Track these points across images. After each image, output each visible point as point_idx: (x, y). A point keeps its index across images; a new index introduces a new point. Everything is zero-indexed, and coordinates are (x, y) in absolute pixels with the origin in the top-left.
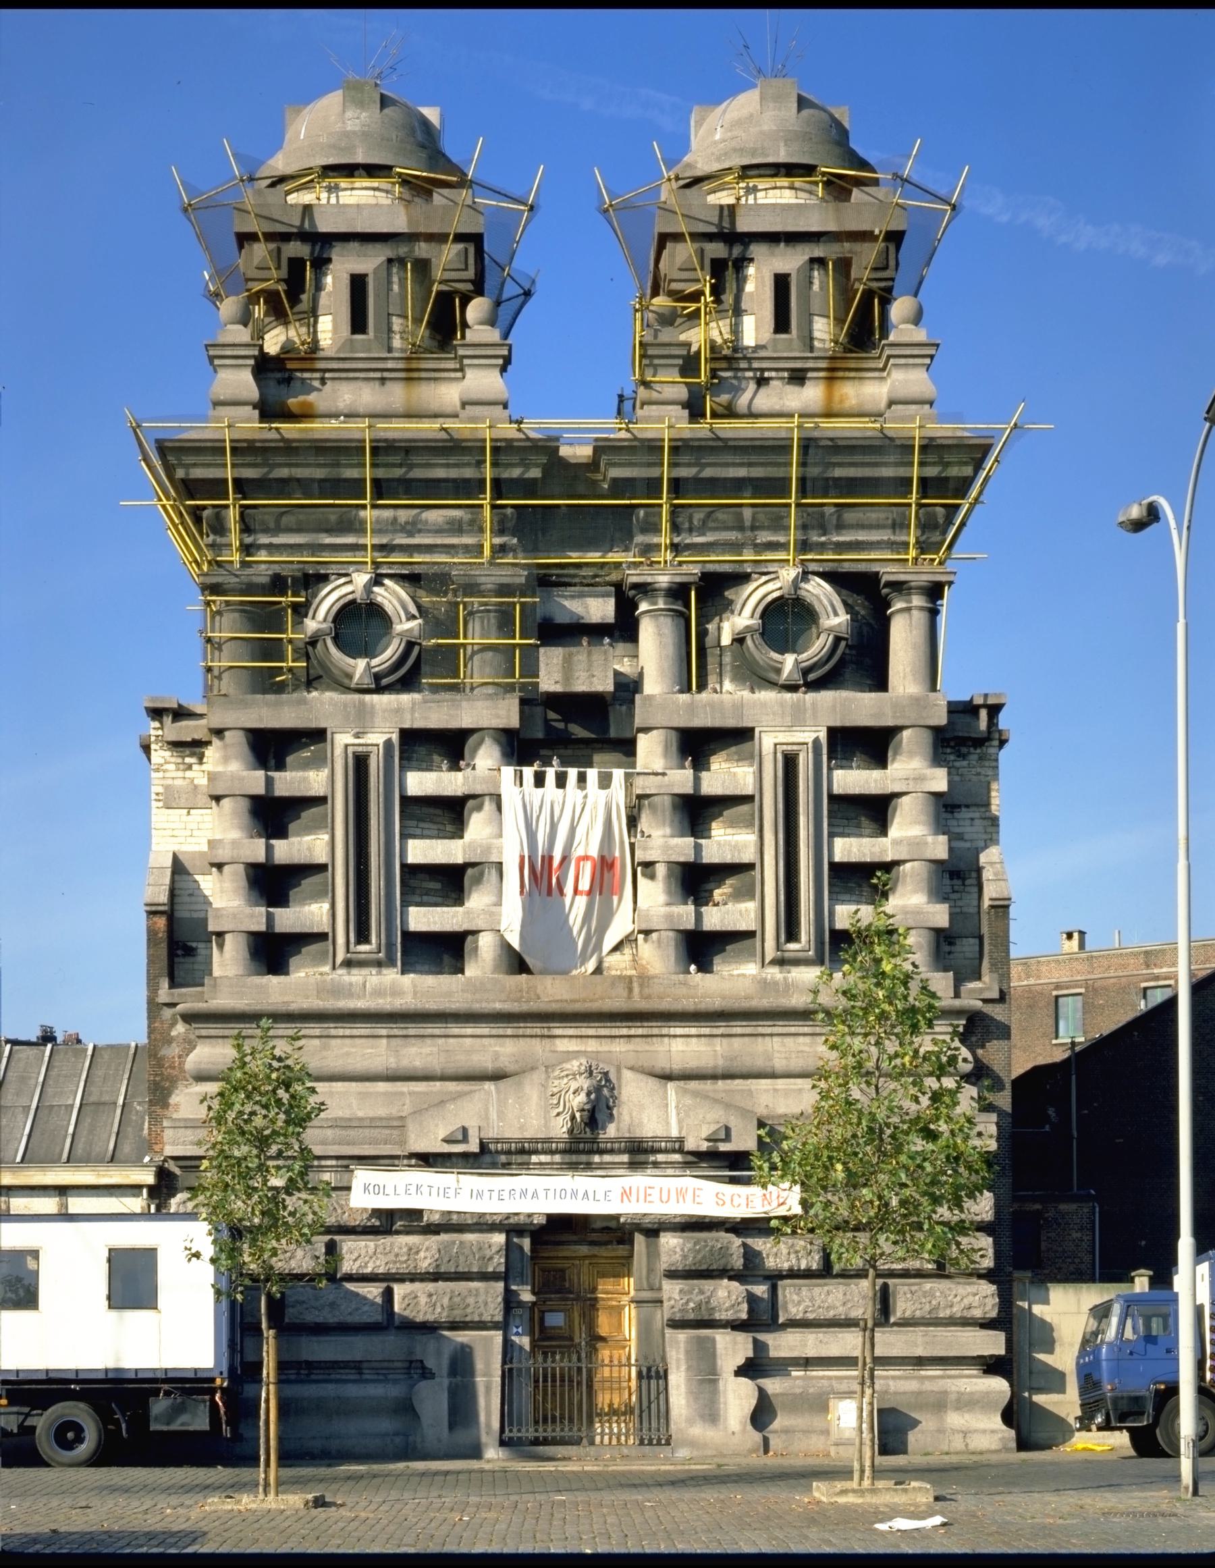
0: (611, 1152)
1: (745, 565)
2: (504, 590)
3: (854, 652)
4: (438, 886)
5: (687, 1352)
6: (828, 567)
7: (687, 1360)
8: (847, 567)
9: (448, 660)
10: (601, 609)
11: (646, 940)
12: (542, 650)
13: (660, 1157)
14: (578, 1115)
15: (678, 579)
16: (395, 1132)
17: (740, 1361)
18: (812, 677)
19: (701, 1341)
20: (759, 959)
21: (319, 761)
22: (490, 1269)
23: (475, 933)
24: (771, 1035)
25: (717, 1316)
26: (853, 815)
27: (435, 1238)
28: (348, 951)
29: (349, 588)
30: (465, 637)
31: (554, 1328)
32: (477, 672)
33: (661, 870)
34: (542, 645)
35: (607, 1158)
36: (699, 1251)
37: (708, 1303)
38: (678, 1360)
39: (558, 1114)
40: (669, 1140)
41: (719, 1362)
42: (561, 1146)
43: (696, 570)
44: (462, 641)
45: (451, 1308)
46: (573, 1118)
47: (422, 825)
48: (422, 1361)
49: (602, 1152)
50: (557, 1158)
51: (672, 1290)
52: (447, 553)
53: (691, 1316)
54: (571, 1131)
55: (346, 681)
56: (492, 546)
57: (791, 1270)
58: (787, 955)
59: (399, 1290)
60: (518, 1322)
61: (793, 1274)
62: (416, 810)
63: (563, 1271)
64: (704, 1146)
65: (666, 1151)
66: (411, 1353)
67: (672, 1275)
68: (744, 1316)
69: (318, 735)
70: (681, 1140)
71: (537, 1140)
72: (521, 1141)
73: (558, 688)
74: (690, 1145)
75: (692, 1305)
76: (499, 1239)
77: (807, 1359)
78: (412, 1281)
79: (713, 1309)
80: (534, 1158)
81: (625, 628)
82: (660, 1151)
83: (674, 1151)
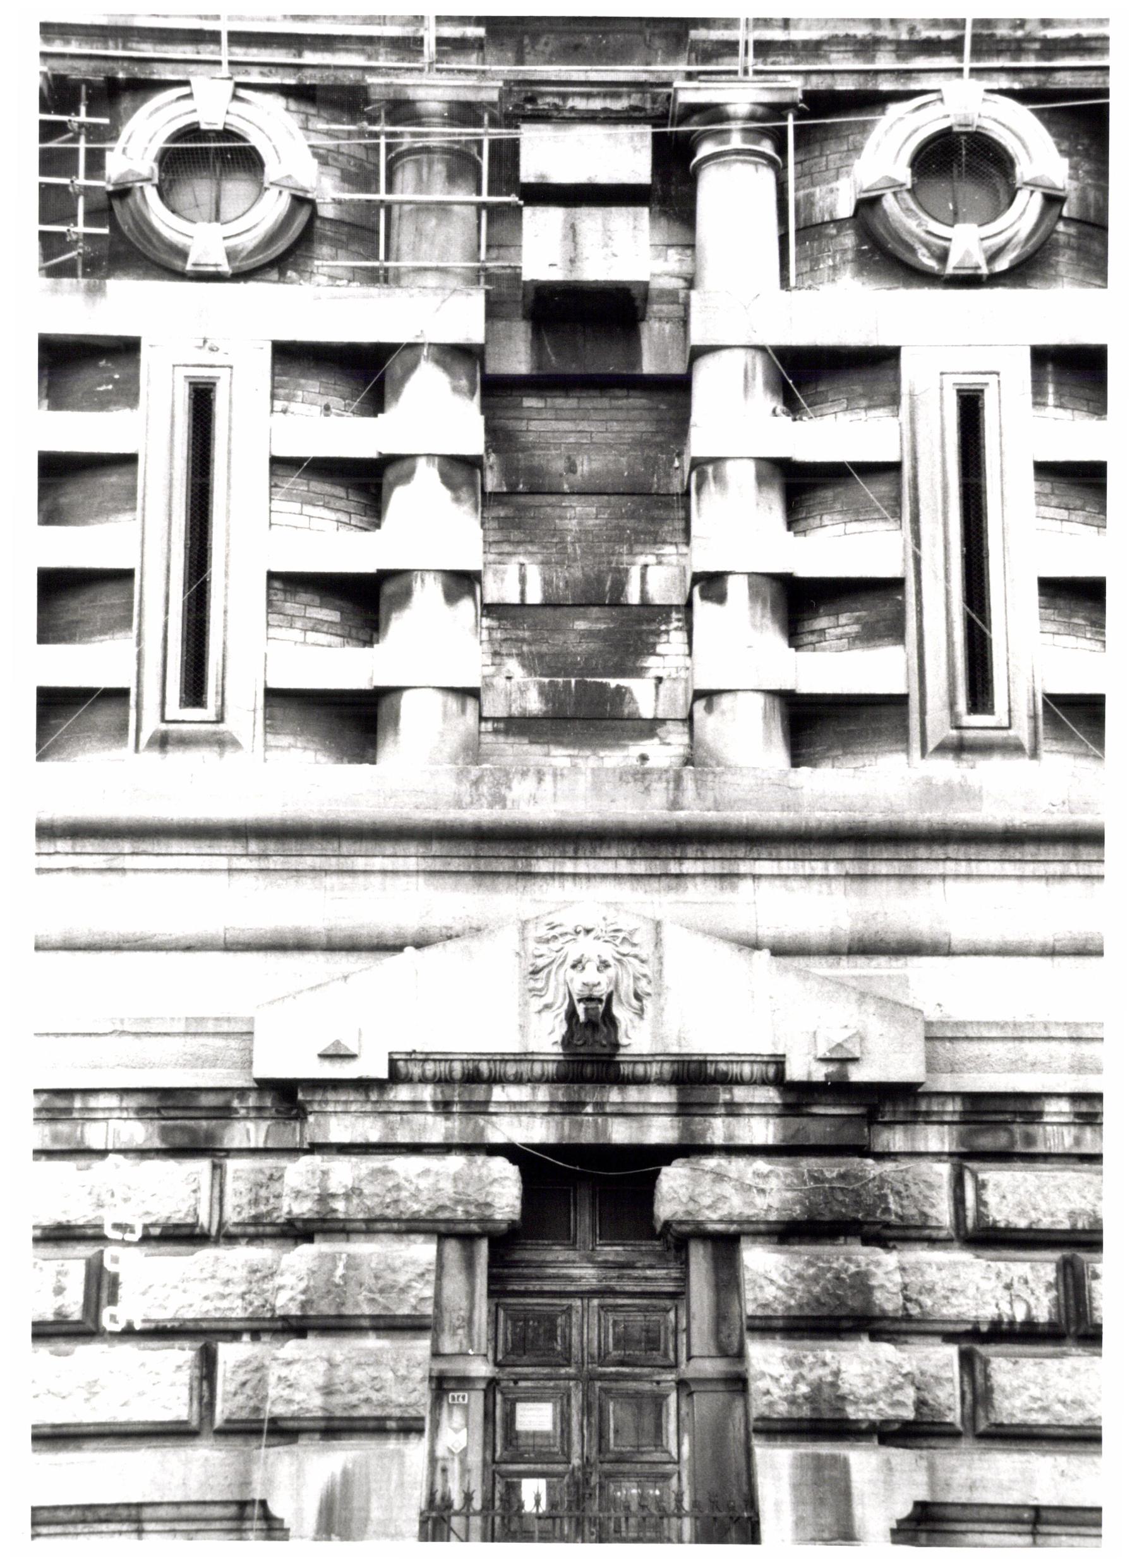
0: (643, 1081)
1: (881, 78)
2: (464, 113)
3: (1072, 230)
4: (334, 616)
5: (796, 1487)
6: (1033, 81)
7: (798, 1502)
8: (1065, 81)
9: (362, 232)
10: (627, 156)
11: (709, 709)
12: (527, 211)
13: (740, 1094)
14: (580, 1008)
15: (767, 98)
16: (234, 1043)
17: (904, 1509)
18: (1002, 265)
19: (819, 1464)
20: (916, 744)
21: (128, 394)
22: (405, 1310)
23: (398, 690)
24: (944, 877)
25: (852, 1412)
26: (1079, 503)
27: (305, 1249)
28: (163, 720)
29: (186, 105)
30: (390, 188)
31: (535, 1434)
32: (412, 247)
33: (737, 588)
34: (526, 204)
35: (633, 1094)
36: (815, 1279)
37: (834, 1385)
38: (777, 1504)
39: (547, 1007)
40: (754, 1059)
41: (858, 1511)
42: (551, 1068)
43: (797, 83)
44: (382, 195)
45: (328, 1390)
46: (571, 1015)
47: (308, 509)
48: (263, 1503)
49: (624, 1081)
50: (543, 1093)
51: (770, 1363)
52: (362, 52)
53: (806, 1412)
54: (567, 1041)
55: (178, 264)
56: (440, 41)
57: (996, 1324)
58: (969, 734)
59: (229, 1354)
60: (458, 1418)
61: (1003, 1333)
62: (295, 482)
63: (551, 1319)
64: (819, 1073)
65: (752, 1082)
66: (246, 1483)
67: (764, 1327)
68: (909, 1414)
69: (126, 349)
70: (779, 1062)
71: (505, 1059)
72: (475, 1059)
73: (557, 275)
74: (795, 1072)
75: (803, 1389)
76: (423, 1251)
77: (1037, 1509)
78: (256, 1334)
79: (843, 1398)
80: (499, 1093)
81: (670, 191)
82: (739, 1081)
83: (764, 1082)
